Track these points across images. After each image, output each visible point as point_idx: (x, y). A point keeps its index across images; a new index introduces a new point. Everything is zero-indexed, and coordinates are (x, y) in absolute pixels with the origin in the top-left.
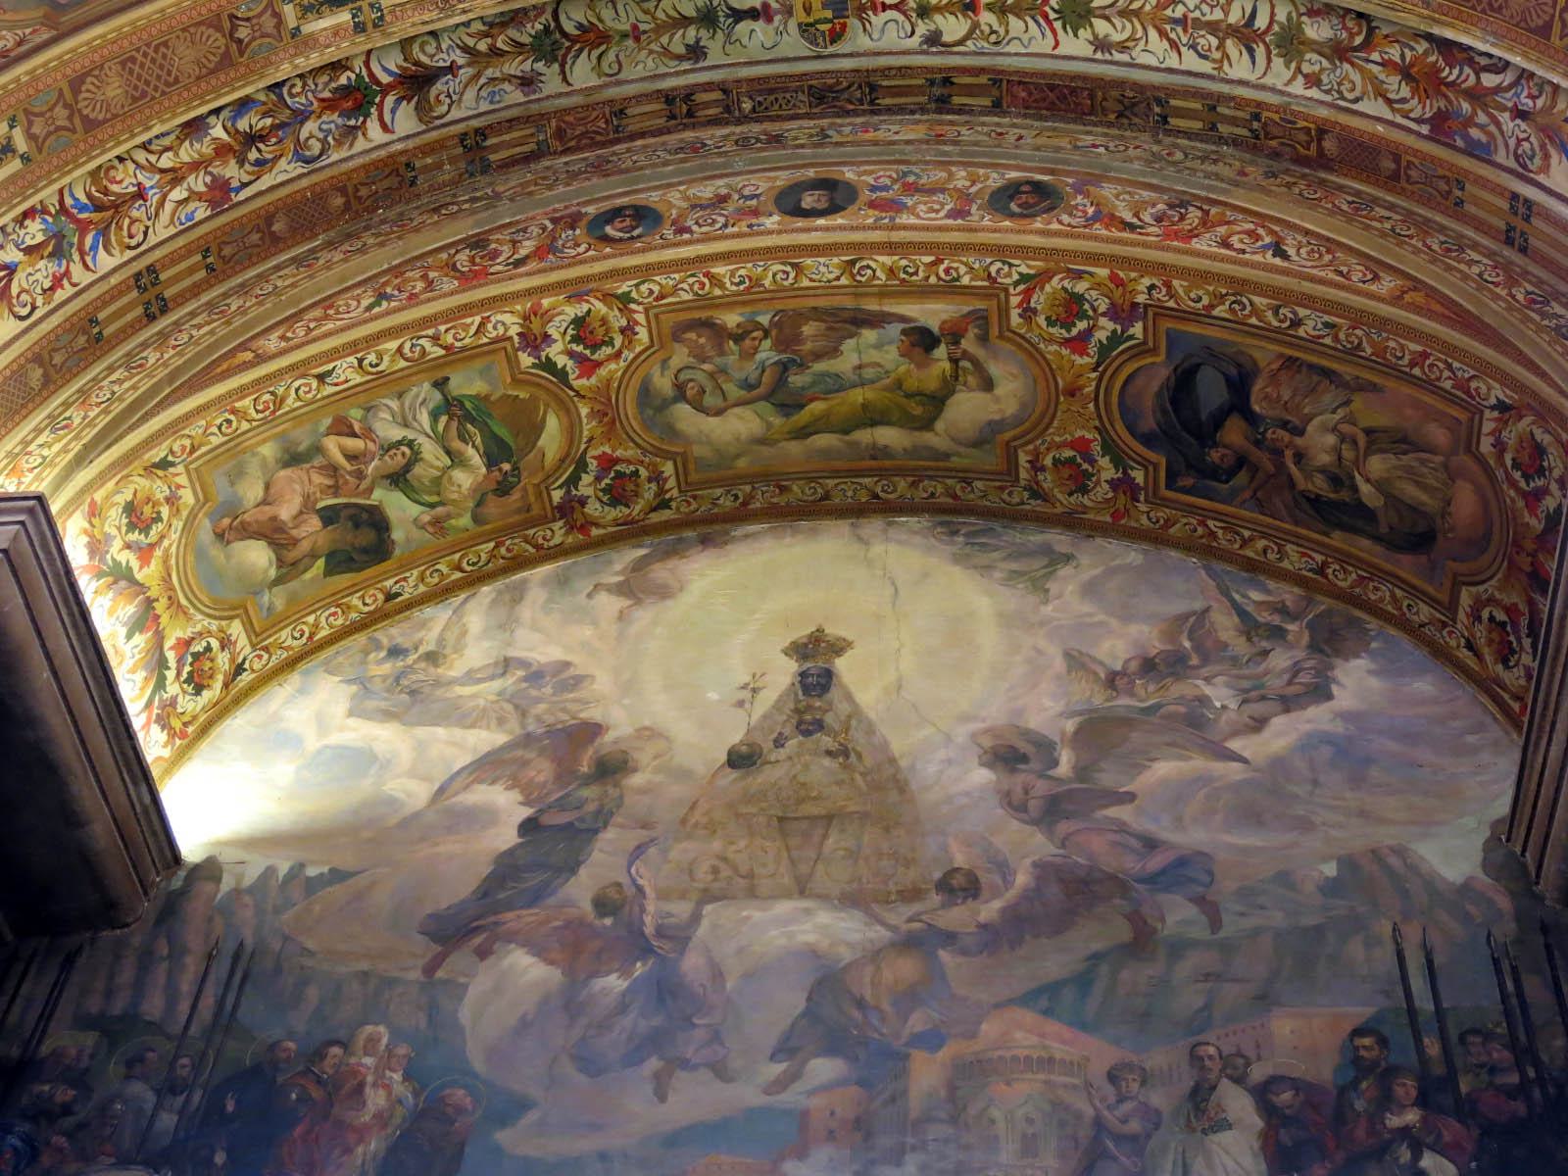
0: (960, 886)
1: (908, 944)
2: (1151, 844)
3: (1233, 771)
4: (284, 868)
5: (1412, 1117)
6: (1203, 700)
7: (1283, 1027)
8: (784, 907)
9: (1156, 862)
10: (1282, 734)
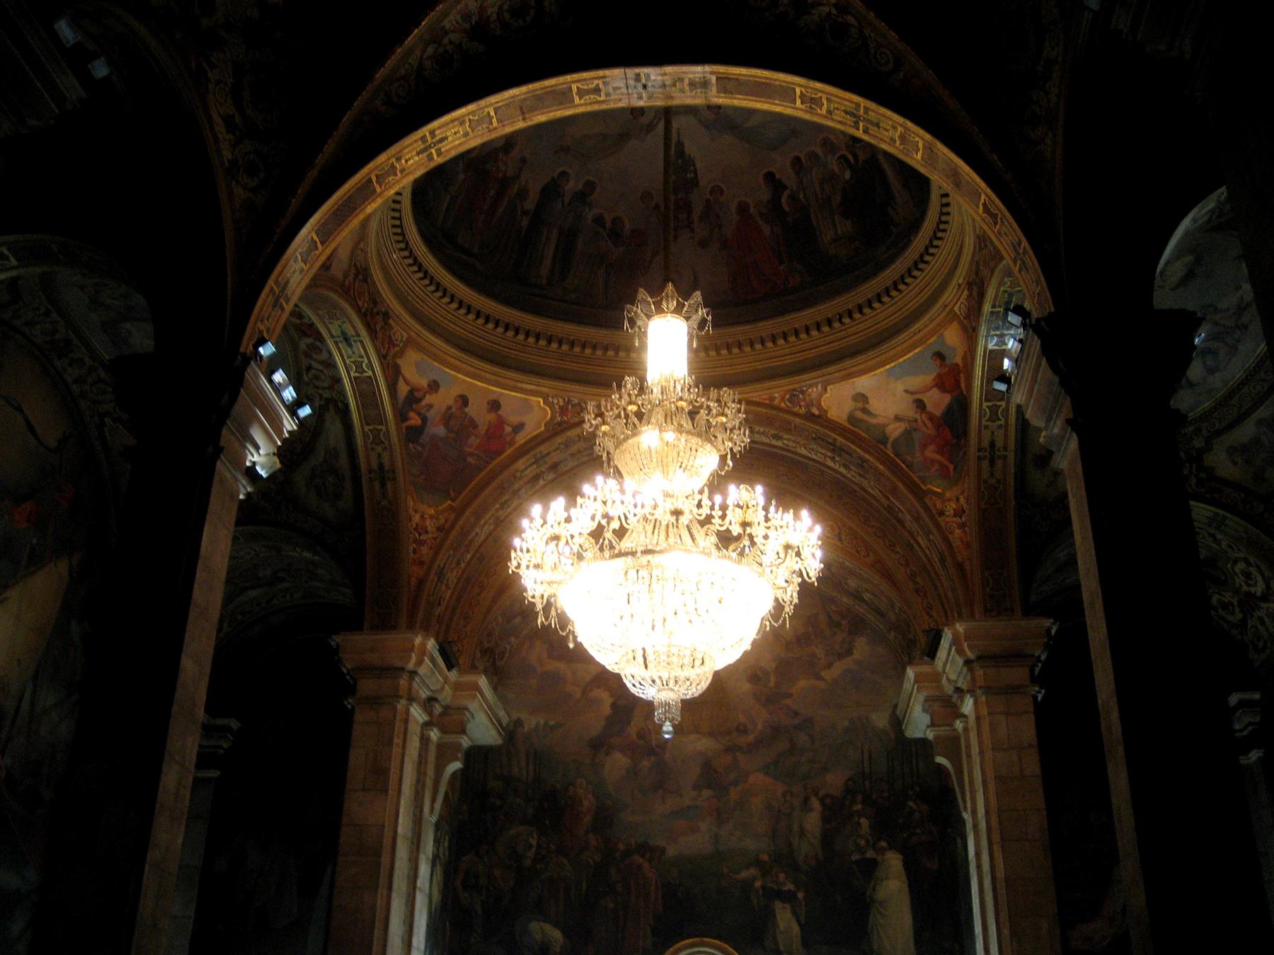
0: (742, 730)
1: (729, 750)
2: (796, 714)
3: (821, 685)
4: (542, 722)
5: (859, 807)
6: (814, 655)
7: (829, 778)
8: (693, 737)
9: (797, 721)
10: (838, 668)
